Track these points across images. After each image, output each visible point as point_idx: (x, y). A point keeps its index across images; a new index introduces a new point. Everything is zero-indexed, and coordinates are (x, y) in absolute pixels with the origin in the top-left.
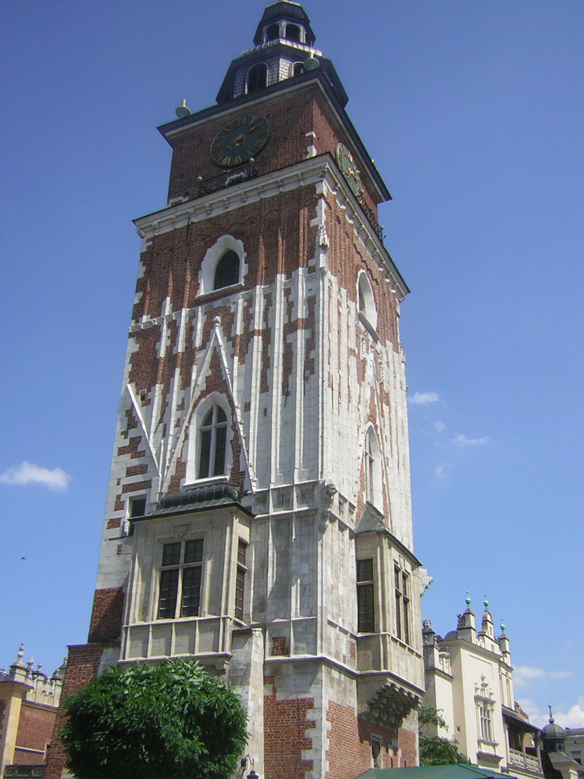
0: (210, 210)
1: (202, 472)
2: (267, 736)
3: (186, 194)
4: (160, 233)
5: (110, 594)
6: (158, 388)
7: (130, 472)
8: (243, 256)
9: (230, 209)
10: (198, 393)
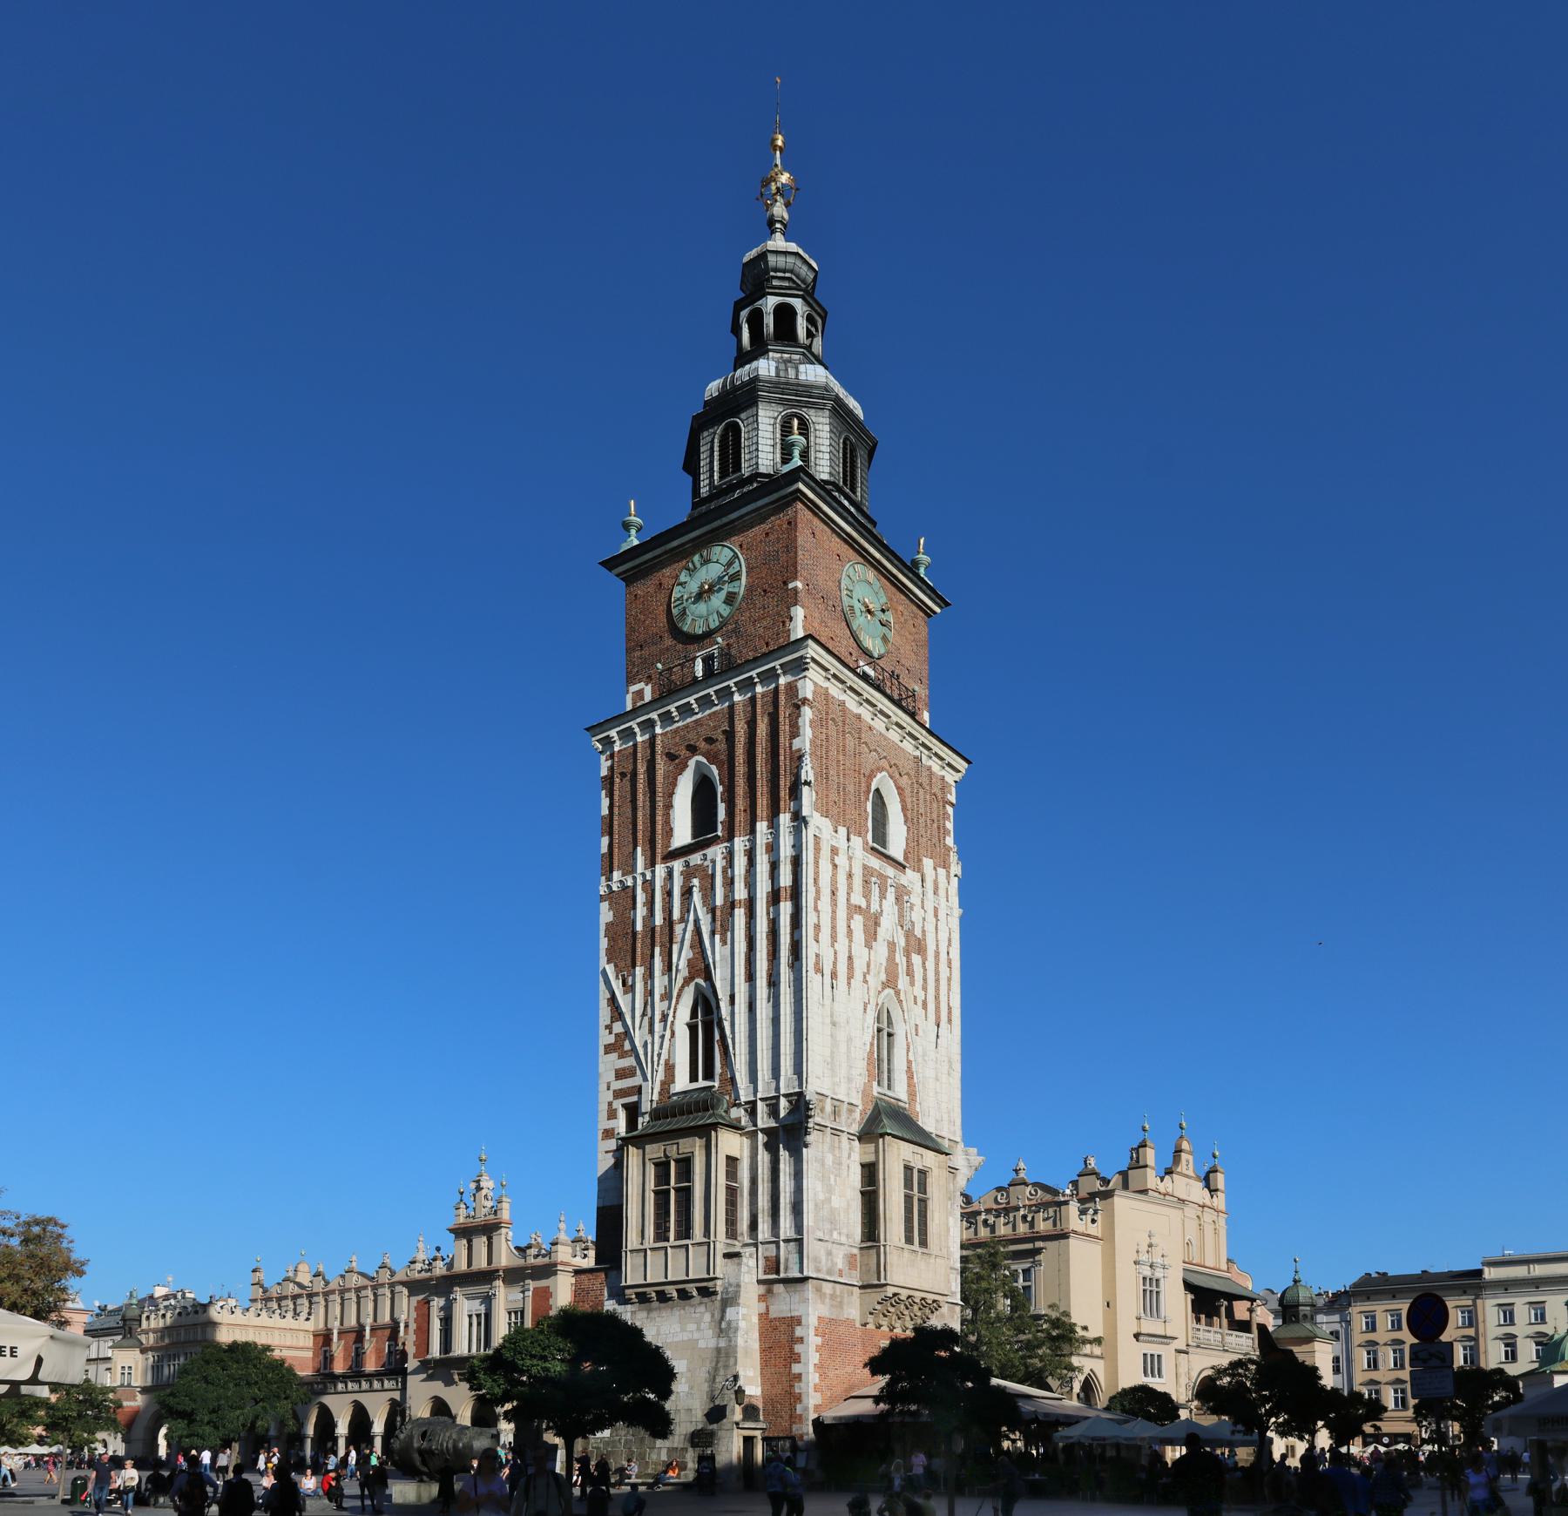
2: (763, 1351)
6: (639, 971)
10: (680, 981)
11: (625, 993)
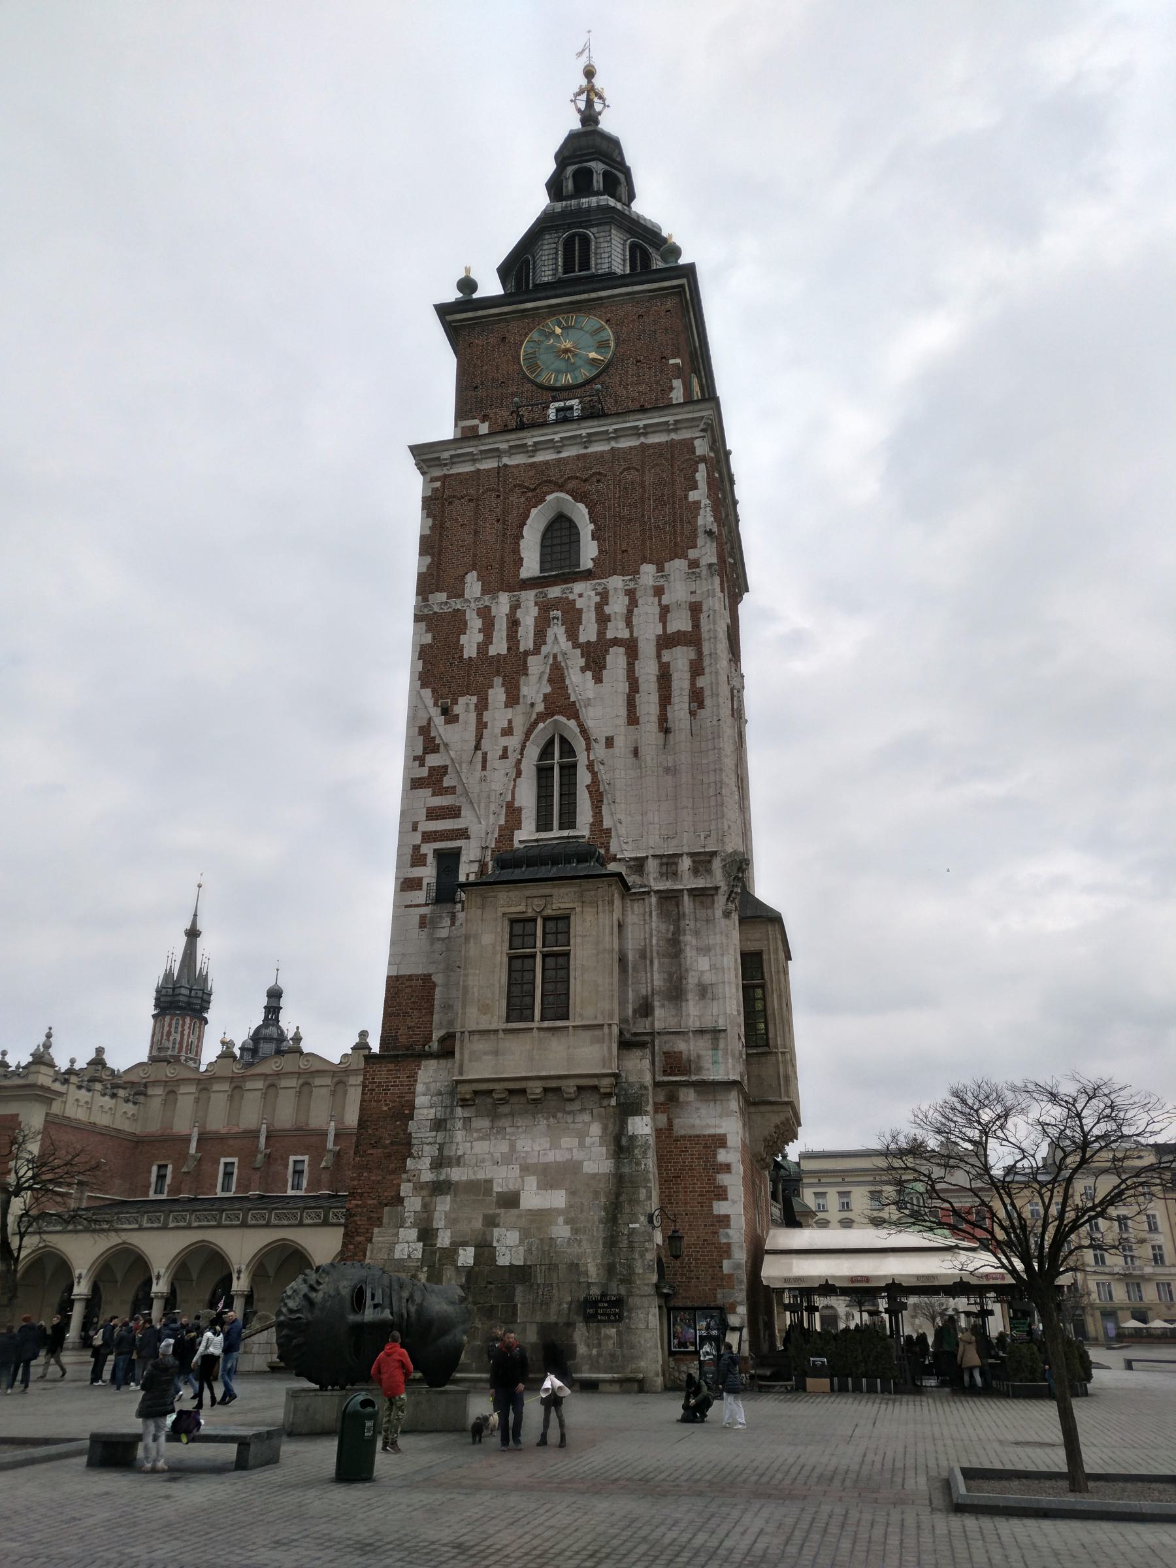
0: (533, 451)
1: (543, 823)
3: (484, 419)
4: (451, 472)
5: (413, 983)
7: (433, 814)
8: (586, 529)
9: (563, 455)
11: (447, 722)
